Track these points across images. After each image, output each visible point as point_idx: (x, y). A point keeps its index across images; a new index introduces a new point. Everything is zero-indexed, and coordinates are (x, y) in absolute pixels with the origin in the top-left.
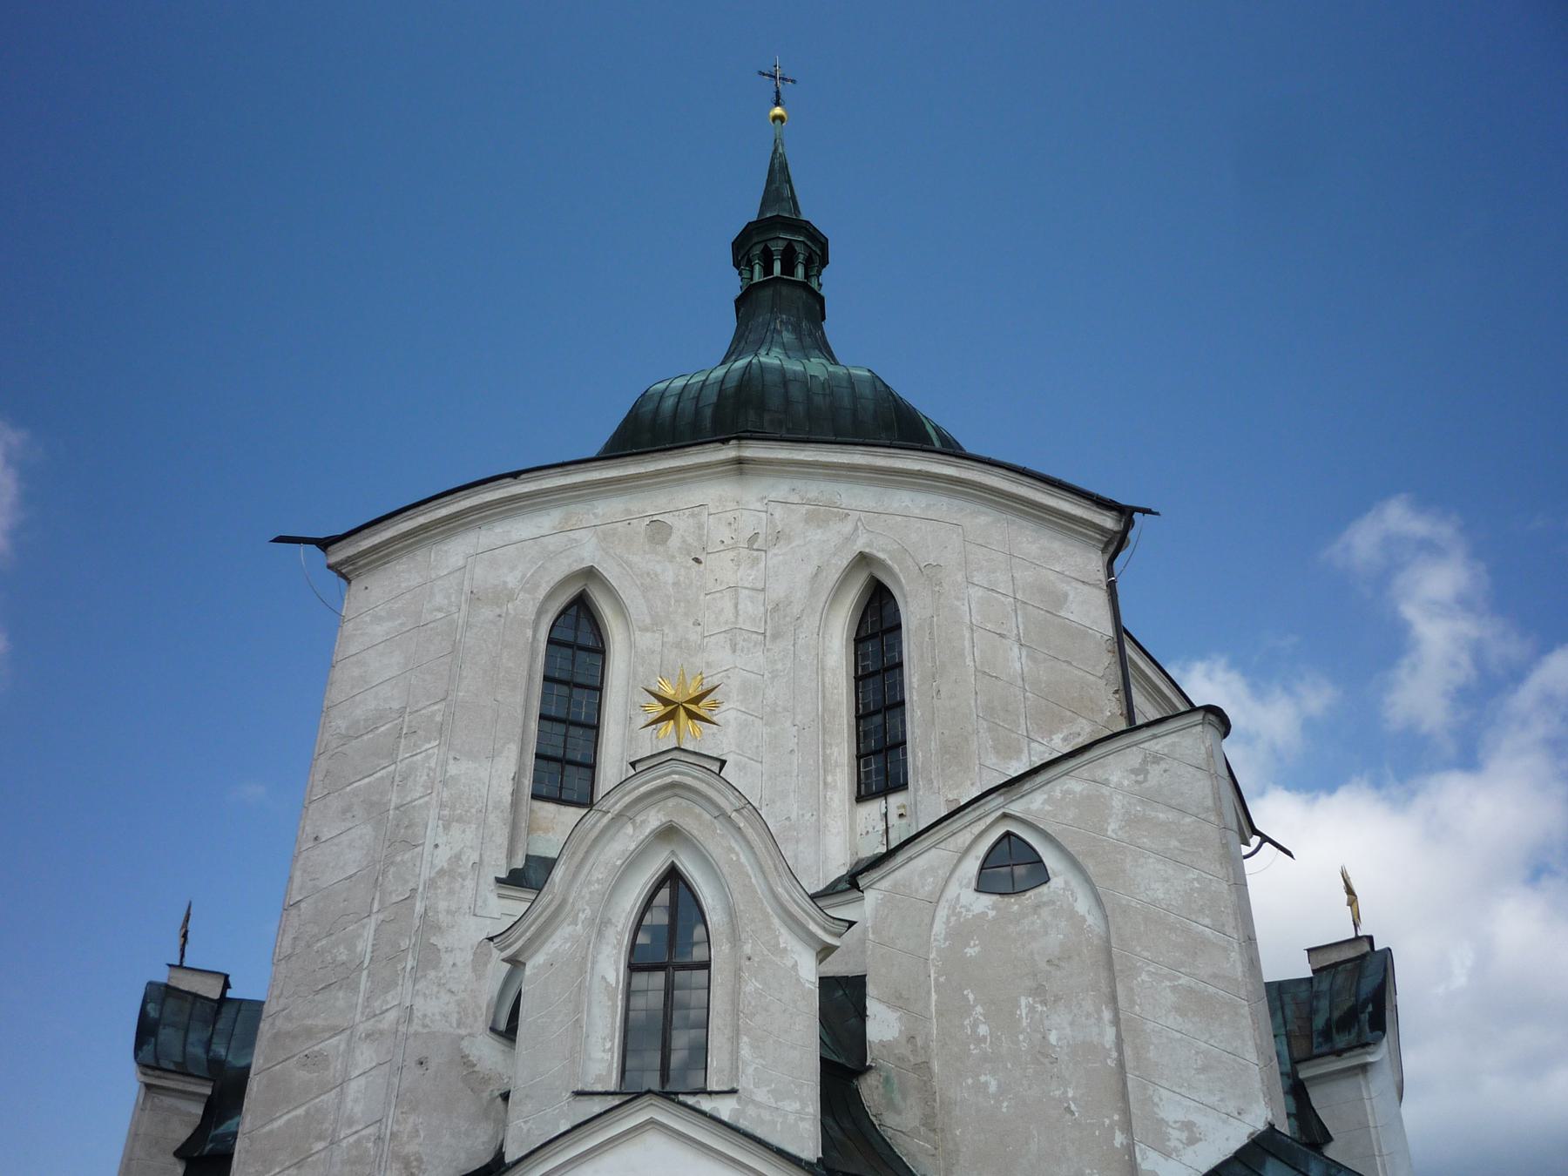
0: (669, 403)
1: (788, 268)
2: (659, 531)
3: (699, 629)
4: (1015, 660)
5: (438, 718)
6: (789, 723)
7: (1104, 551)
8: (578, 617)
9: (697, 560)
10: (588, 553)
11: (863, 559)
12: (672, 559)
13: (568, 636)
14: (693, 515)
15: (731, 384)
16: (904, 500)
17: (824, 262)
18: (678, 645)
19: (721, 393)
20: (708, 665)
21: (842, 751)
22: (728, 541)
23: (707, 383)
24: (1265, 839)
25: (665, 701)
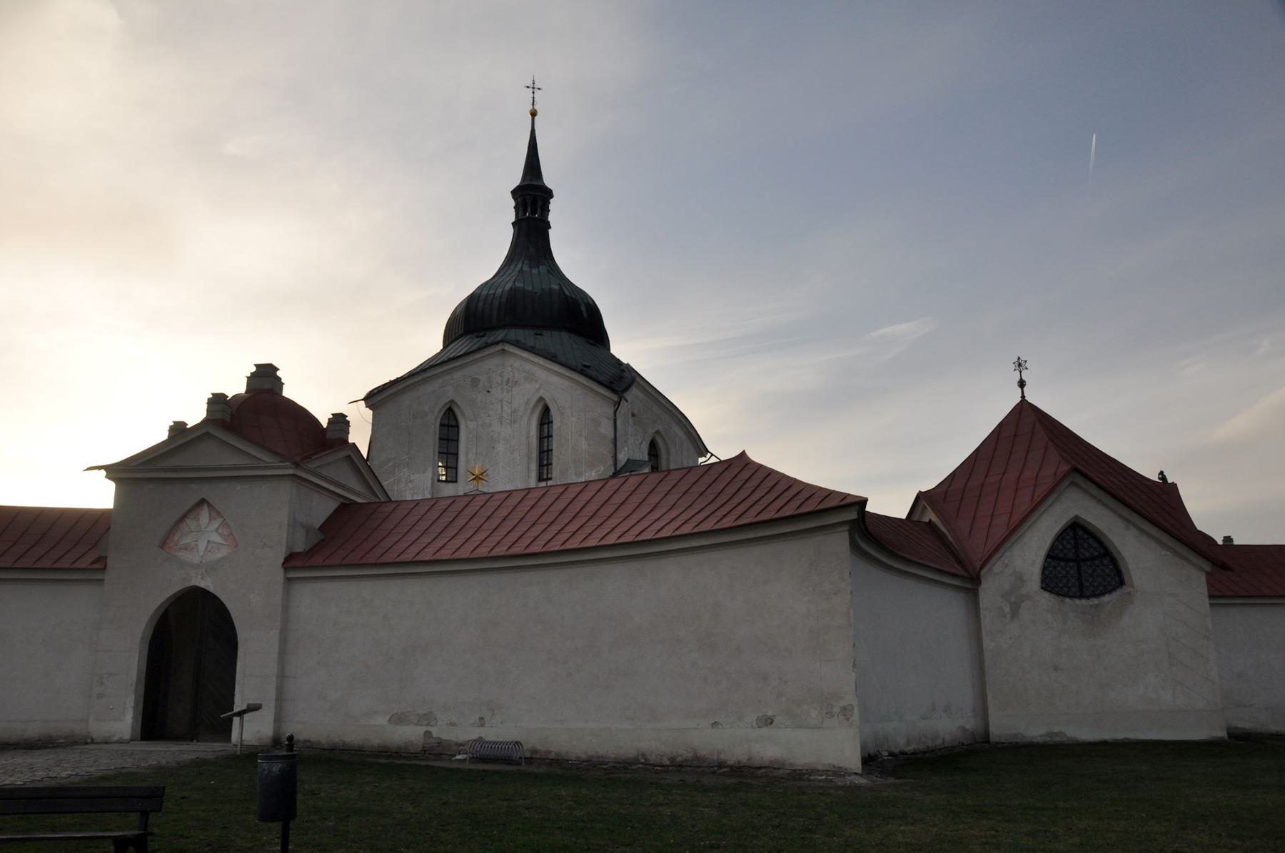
0: (481, 304)
1: (534, 212)
2: (475, 382)
3: (489, 418)
4: (584, 445)
5: (407, 460)
6: (517, 455)
7: (615, 406)
8: (449, 414)
9: (488, 392)
10: (450, 394)
11: (541, 399)
12: (479, 392)
13: (446, 422)
14: (487, 373)
15: (504, 300)
16: (555, 379)
17: (552, 196)
18: (482, 425)
19: (500, 302)
20: (493, 431)
21: (534, 467)
22: (499, 382)
23: (496, 295)
24: (712, 455)
25: (473, 475)
